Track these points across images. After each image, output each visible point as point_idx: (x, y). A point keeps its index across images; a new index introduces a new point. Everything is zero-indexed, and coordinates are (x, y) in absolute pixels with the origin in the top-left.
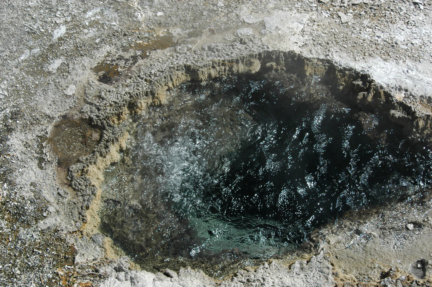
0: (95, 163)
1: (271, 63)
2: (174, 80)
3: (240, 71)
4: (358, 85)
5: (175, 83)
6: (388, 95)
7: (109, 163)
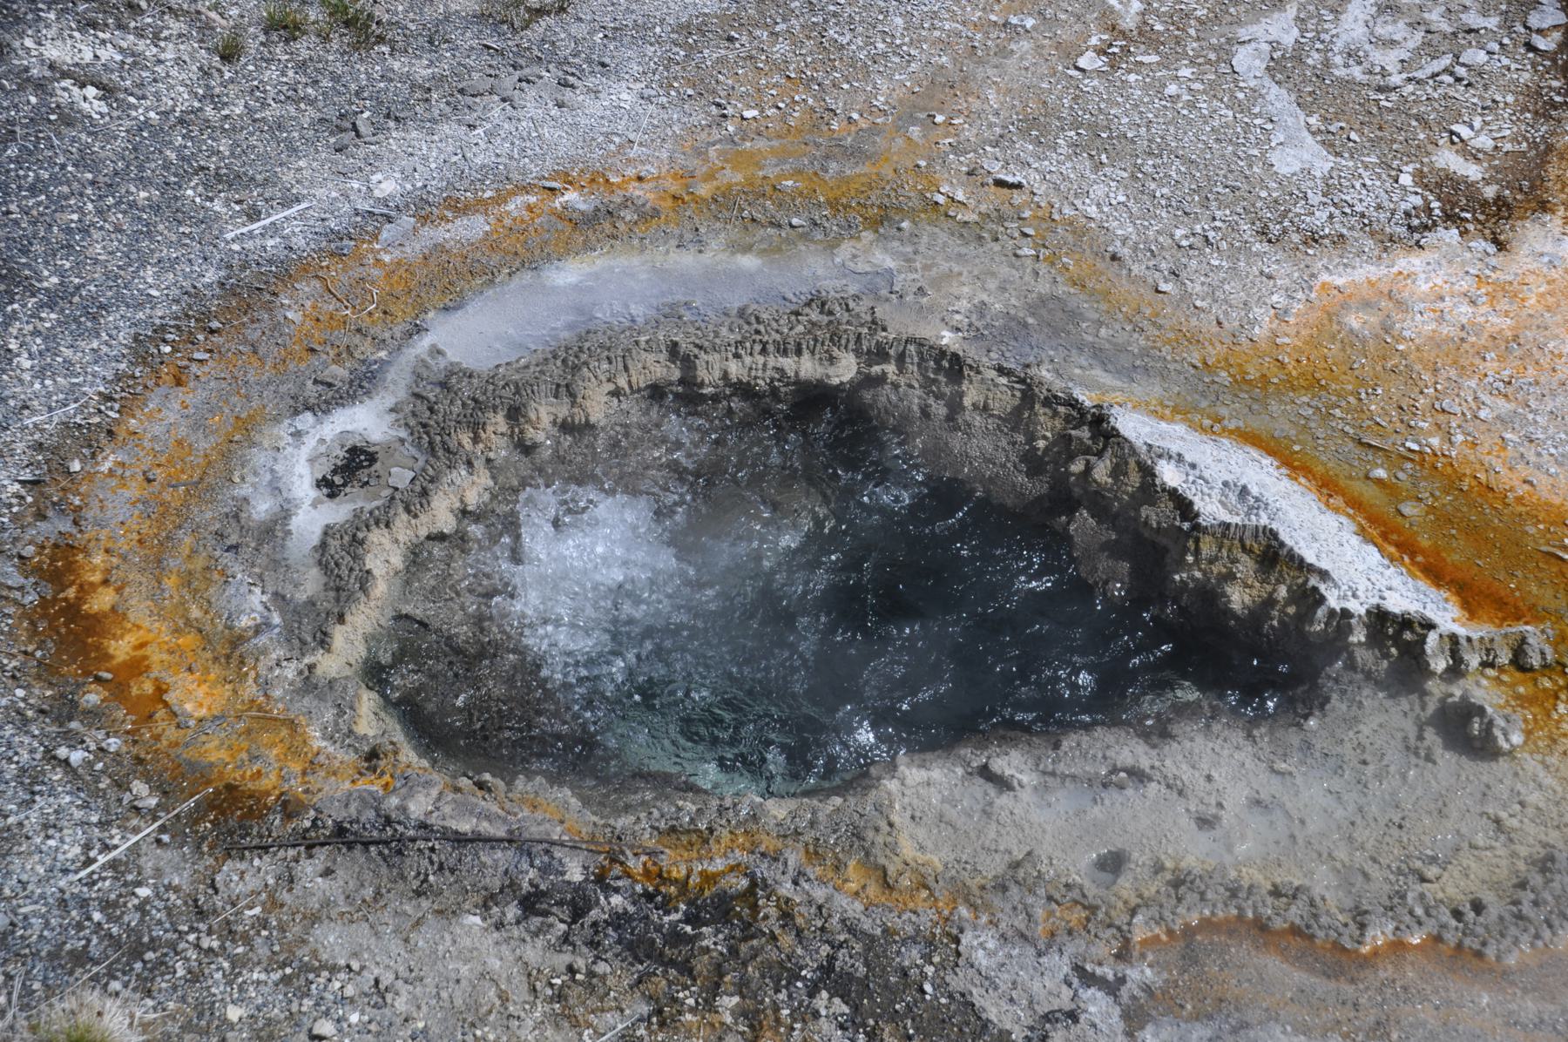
0: (387, 526)
1: (884, 366)
2: (632, 372)
3: (802, 374)
4: (1080, 439)
5: (634, 380)
6: (1148, 472)
7: (423, 532)
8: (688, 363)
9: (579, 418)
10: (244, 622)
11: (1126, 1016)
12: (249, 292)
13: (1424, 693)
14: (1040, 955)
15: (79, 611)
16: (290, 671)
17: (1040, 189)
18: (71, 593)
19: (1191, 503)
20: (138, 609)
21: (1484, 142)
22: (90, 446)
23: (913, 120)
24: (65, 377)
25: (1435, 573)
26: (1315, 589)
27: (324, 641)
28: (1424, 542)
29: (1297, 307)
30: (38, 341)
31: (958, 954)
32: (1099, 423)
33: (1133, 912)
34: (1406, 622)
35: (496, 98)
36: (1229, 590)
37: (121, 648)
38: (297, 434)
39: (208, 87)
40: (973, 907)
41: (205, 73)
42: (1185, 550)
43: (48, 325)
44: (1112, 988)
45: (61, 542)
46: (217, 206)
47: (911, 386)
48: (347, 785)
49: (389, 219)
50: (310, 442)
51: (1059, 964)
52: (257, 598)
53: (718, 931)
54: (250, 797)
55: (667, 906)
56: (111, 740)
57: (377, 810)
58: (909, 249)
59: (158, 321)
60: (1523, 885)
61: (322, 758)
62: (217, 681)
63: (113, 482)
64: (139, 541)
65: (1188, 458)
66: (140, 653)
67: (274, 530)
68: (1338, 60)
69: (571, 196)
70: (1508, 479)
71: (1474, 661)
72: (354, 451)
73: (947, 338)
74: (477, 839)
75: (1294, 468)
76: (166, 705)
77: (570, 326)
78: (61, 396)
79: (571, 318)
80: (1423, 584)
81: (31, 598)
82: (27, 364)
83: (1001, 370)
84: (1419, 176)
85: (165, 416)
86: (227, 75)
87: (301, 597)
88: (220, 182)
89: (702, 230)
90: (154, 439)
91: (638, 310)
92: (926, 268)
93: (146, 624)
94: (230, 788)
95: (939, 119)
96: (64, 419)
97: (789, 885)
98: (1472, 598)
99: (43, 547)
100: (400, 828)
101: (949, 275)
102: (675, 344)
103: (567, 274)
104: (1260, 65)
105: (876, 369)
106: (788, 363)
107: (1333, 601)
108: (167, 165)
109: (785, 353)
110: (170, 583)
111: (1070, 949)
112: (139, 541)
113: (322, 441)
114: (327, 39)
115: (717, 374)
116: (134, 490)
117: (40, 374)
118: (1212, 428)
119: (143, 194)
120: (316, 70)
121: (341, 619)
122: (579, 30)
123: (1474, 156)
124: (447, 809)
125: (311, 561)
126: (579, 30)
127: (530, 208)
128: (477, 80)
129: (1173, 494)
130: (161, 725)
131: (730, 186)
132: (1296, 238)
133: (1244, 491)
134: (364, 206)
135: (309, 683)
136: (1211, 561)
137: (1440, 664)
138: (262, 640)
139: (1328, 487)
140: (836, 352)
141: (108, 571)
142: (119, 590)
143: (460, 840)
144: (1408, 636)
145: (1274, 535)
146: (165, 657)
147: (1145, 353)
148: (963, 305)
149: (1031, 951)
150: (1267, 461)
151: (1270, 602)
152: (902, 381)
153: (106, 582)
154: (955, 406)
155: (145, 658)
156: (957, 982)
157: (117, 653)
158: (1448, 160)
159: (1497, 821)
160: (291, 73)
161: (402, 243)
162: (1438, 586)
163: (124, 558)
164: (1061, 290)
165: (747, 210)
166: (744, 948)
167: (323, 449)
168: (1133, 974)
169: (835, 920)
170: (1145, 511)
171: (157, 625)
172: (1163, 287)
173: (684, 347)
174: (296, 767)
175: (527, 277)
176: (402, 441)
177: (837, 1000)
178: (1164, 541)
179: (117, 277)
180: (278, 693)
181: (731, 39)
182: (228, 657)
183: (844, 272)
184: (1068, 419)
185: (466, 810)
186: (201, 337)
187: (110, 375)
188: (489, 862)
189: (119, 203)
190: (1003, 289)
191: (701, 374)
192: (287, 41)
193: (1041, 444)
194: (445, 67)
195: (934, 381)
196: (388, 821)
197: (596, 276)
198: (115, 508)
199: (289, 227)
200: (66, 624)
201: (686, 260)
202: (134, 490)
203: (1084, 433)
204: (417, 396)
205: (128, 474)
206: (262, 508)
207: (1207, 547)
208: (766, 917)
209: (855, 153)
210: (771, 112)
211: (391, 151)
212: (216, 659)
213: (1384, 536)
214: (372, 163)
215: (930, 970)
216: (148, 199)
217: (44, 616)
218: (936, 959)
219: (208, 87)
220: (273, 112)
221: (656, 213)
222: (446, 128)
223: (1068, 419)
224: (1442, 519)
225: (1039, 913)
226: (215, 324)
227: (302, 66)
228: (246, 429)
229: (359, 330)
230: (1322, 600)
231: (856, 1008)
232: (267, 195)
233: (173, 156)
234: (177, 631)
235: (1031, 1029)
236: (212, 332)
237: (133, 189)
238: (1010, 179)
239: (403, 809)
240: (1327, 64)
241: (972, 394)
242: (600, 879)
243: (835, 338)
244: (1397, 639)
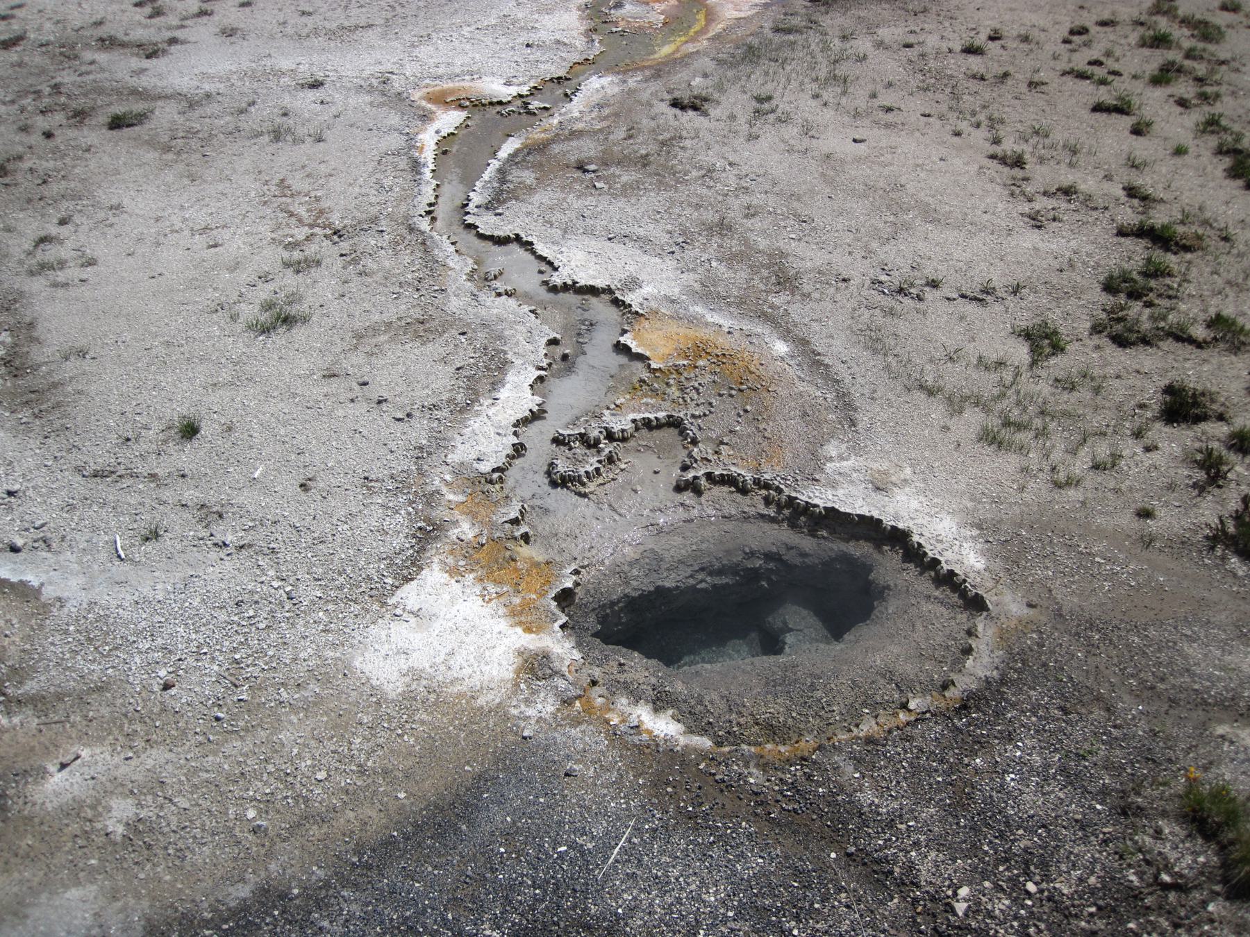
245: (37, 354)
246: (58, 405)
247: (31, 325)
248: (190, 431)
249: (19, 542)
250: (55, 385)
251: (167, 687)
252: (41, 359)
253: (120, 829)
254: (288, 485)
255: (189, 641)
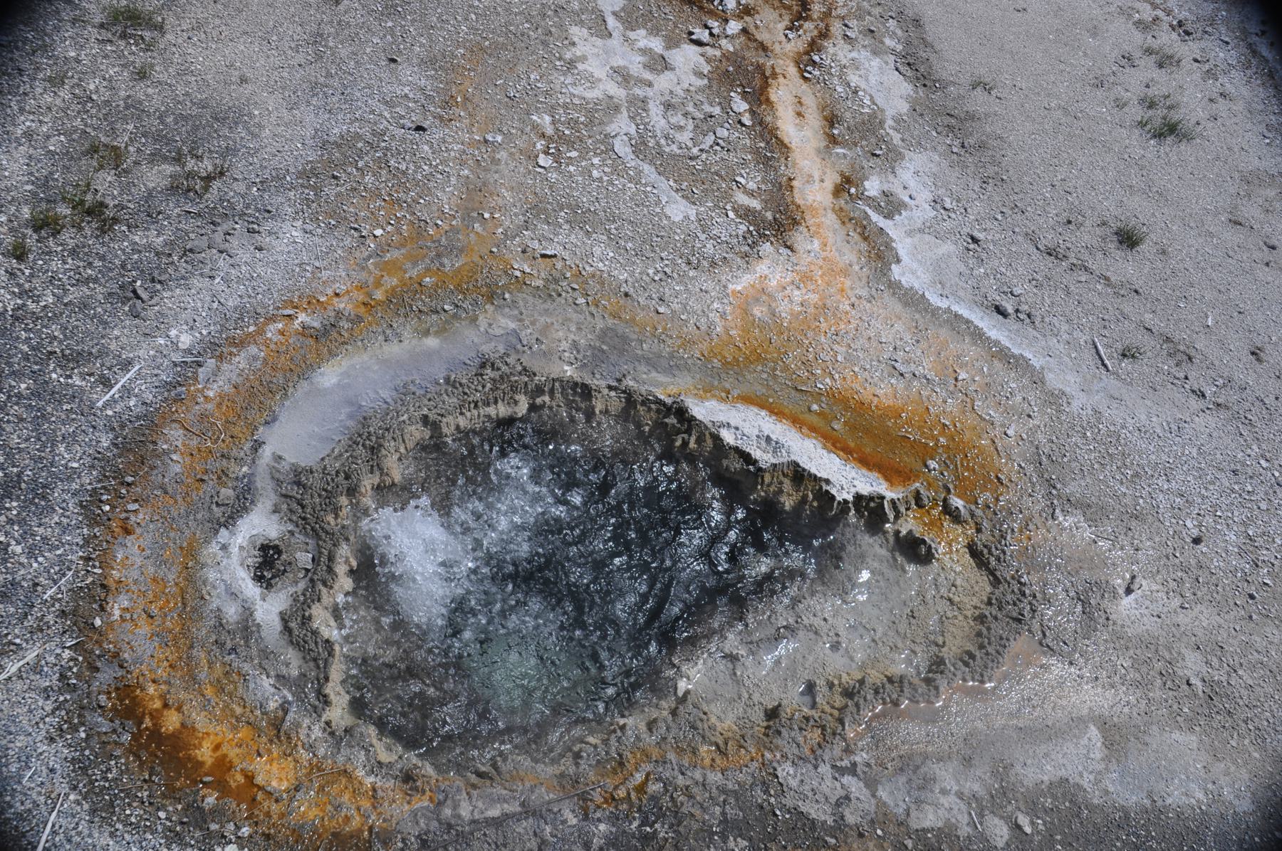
6: (717, 438)
8: (435, 426)
9: (388, 481)
10: (272, 705)
11: (867, 786)
12: (135, 448)
13: (885, 533)
14: (816, 767)
15: (160, 734)
16: (317, 732)
17: (566, 255)
18: (147, 723)
19: (749, 454)
20: (200, 720)
21: (752, 185)
22: (95, 601)
23: (474, 220)
24: (50, 551)
25: (865, 462)
26: (827, 491)
27: (327, 702)
28: (852, 445)
29: (728, 309)
30: (16, 528)
31: (782, 785)
32: (681, 412)
33: (841, 721)
34: (871, 498)
35: (215, 251)
36: (782, 500)
37: (205, 753)
38: (224, 547)
39: (19, 285)
40: (770, 750)
41: (12, 274)
42: (757, 484)
43: (15, 512)
44: (852, 770)
45: (121, 685)
46: (77, 381)
47: (559, 406)
48: (407, 807)
49: (200, 365)
50: (235, 550)
51: (825, 769)
52: (266, 683)
53: (663, 824)
54: (352, 837)
55: (628, 818)
56: (244, 830)
57: (439, 821)
58: (516, 312)
59: (89, 487)
60: (979, 634)
61: (380, 793)
62: (280, 757)
63: (128, 625)
64: (171, 666)
65: (733, 424)
66: (218, 753)
67: (247, 627)
68: (663, 142)
69: (302, 317)
70: (866, 395)
71: (903, 509)
72: (264, 548)
73: (569, 371)
74: (506, 816)
75: (776, 414)
76: (260, 788)
77: (350, 416)
78: (57, 568)
79: (348, 410)
80: (864, 471)
81: (126, 738)
82: (18, 549)
83: (610, 388)
84: (734, 209)
85: (132, 558)
86: (27, 272)
87: (295, 673)
88: (68, 360)
89: (395, 325)
90: (136, 582)
91: (386, 394)
92: (533, 323)
93: (211, 730)
94: (334, 834)
95: (487, 215)
96: (69, 587)
97: (681, 777)
98: (890, 473)
99: (109, 693)
100: (459, 828)
101: (547, 327)
102: (426, 417)
103: (329, 376)
104: (628, 150)
105: (539, 401)
106: (491, 411)
107: (839, 498)
108: (26, 357)
109: (488, 405)
110: (209, 692)
111: (826, 758)
112: (171, 666)
113: (241, 548)
114: (80, 229)
115: (453, 428)
116: (144, 629)
117: (31, 553)
118: (726, 397)
119: (23, 386)
120: (86, 254)
121: (327, 679)
122: (240, 187)
123: (751, 194)
124: (480, 804)
125: (283, 642)
126: (240, 187)
127: (282, 333)
128: (195, 242)
129: (737, 450)
130: (266, 804)
131: (393, 289)
132: (705, 263)
133: (768, 439)
134: (177, 358)
135: (337, 737)
136: (769, 486)
137: (891, 516)
138: (291, 716)
139: (797, 422)
140: (517, 397)
141: (163, 697)
142: (179, 709)
143: (497, 823)
144: (872, 504)
145: (796, 464)
146: (237, 750)
147: (672, 357)
148: (564, 345)
149: (810, 767)
150: (763, 413)
151: (804, 500)
152: (554, 404)
153: (166, 706)
154: (590, 415)
155: (225, 756)
156: (789, 802)
157: (205, 758)
158: (742, 199)
159: (950, 600)
160: (70, 261)
161: (218, 382)
162: (870, 470)
163: (168, 683)
164: (610, 322)
165: (404, 304)
166: (681, 829)
167: (245, 554)
168: (858, 759)
169: (714, 790)
170: (725, 463)
171: (218, 728)
172: (661, 310)
173: (432, 416)
174: (365, 804)
175: (304, 386)
176: (291, 533)
177: (739, 839)
178: (738, 477)
179: (41, 458)
180: (321, 752)
181: (335, 177)
182: (278, 737)
183: (489, 337)
184: (658, 411)
185: (494, 801)
186: (123, 491)
187: (80, 540)
188: (522, 831)
189: (9, 397)
190: (579, 329)
191: (445, 430)
192: (54, 235)
193: (647, 428)
194: (168, 234)
195: (573, 401)
196: (450, 826)
197: (346, 374)
198: (142, 647)
199: (134, 387)
200: (158, 747)
201: (393, 349)
202: (144, 629)
203: (672, 420)
204: (286, 496)
205: (135, 616)
206: (232, 612)
207: (767, 479)
208: (682, 804)
209: (451, 250)
210: (389, 228)
211: (170, 309)
212: (271, 741)
213: (834, 445)
214: (162, 324)
215: (772, 800)
216: (28, 388)
217: (140, 746)
218: (772, 792)
219: (19, 285)
220: (74, 294)
221: (359, 319)
222: (196, 282)
223: (658, 411)
224: (852, 427)
225: (801, 740)
226: (129, 479)
227: (74, 253)
228: (191, 552)
229: (223, 456)
230: (833, 497)
231: (750, 840)
232: (108, 364)
233: (25, 348)
234: (235, 729)
235: (834, 815)
236: (129, 484)
237: (14, 383)
238: (549, 253)
239: (459, 816)
240: (658, 144)
241: (599, 406)
242: (586, 817)
243: (514, 388)
244: (867, 507)
245: (945, 69)
246: (982, 146)
247: (917, 22)
248: (1128, 239)
249: (1010, 310)
250: (971, 117)
251: (1197, 541)
252: (944, 75)
253: (1199, 684)
254: (1239, 345)
255: (1203, 497)
